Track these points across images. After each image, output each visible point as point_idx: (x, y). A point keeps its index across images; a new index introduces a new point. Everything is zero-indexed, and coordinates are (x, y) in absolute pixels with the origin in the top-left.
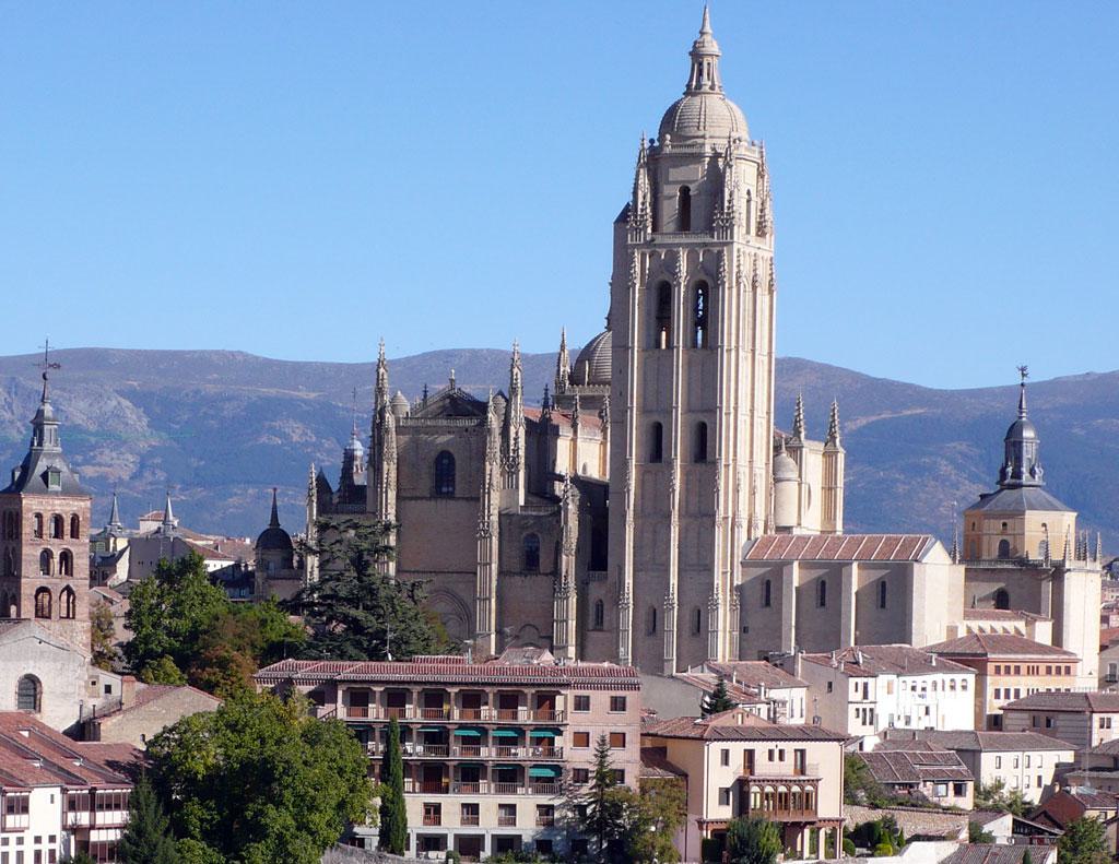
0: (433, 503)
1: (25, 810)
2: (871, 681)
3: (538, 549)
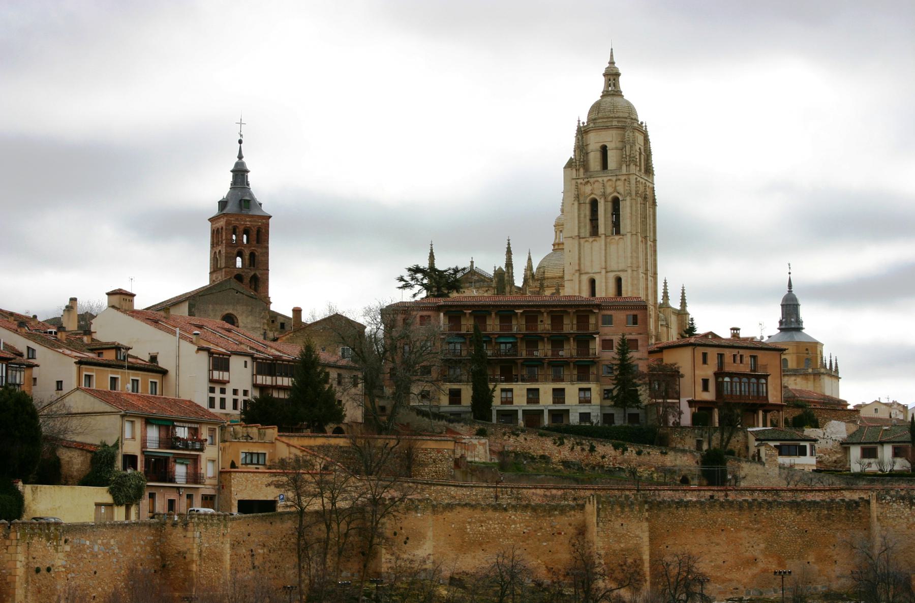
1: (227, 369)
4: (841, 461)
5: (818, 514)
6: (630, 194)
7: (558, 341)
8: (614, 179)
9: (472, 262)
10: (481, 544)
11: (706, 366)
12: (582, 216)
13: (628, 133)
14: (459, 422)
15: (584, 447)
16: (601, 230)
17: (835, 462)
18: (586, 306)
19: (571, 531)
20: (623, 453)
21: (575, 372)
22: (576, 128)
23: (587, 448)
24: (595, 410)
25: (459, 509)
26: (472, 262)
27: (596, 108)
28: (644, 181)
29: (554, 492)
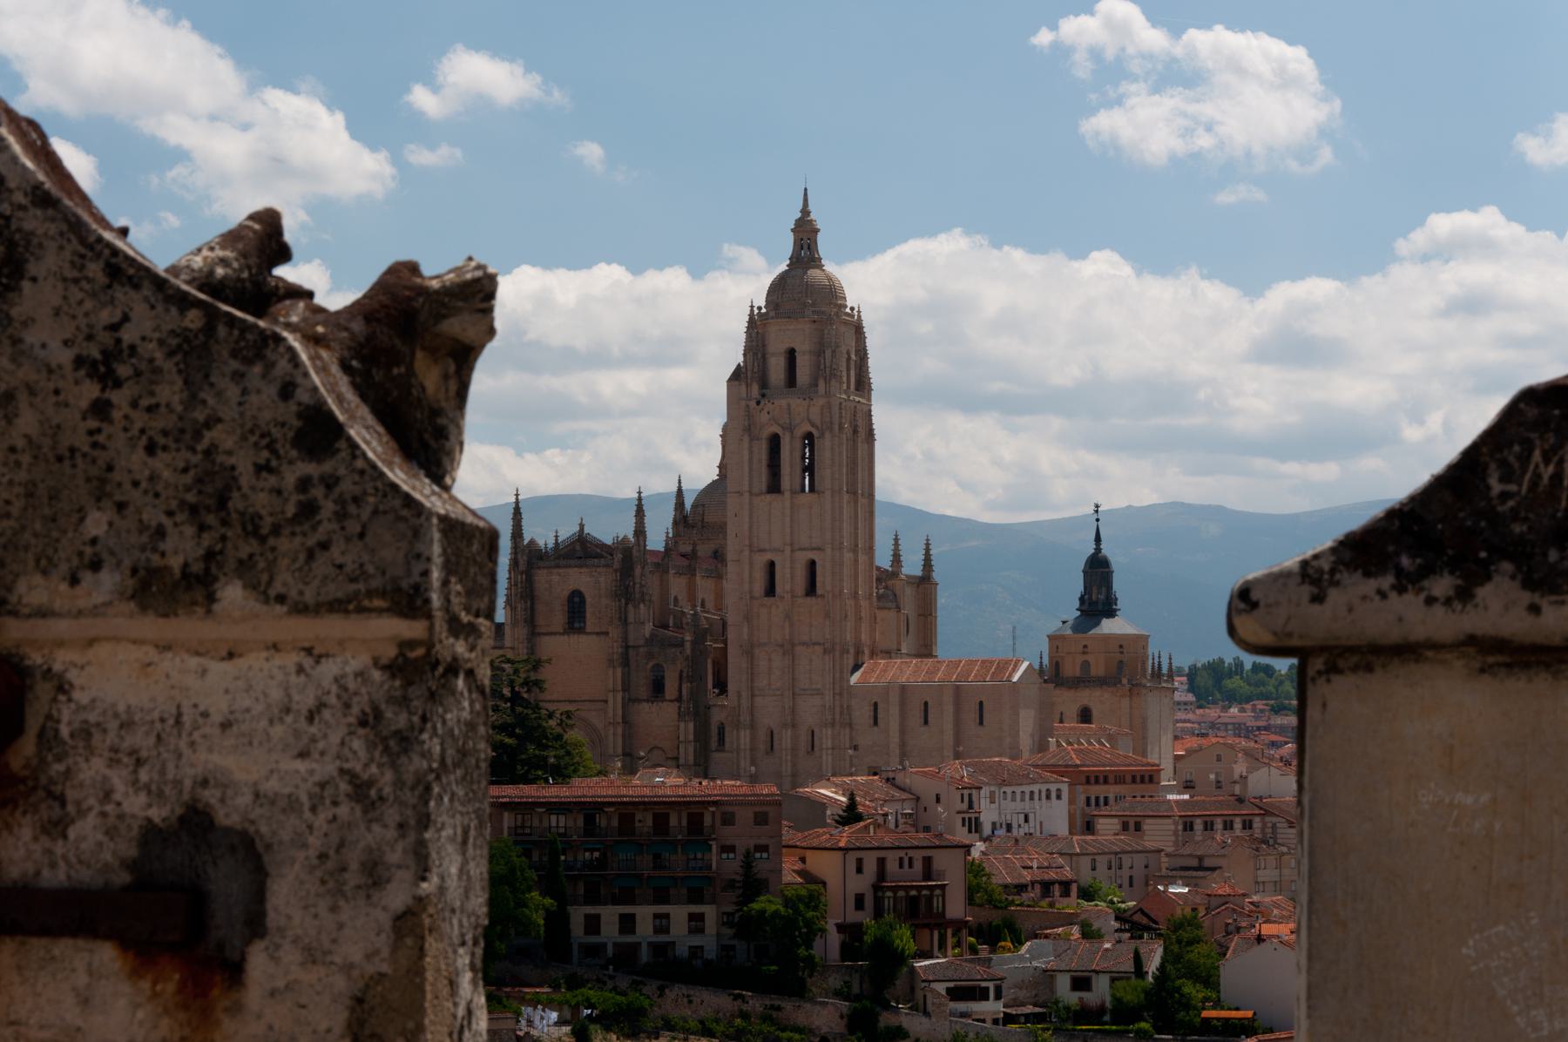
0: (566, 637)
2: (974, 791)
3: (663, 677)
6: (831, 429)
9: (582, 526)
16: (786, 482)
22: (747, 318)
24: (709, 942)
26: (582, 526)
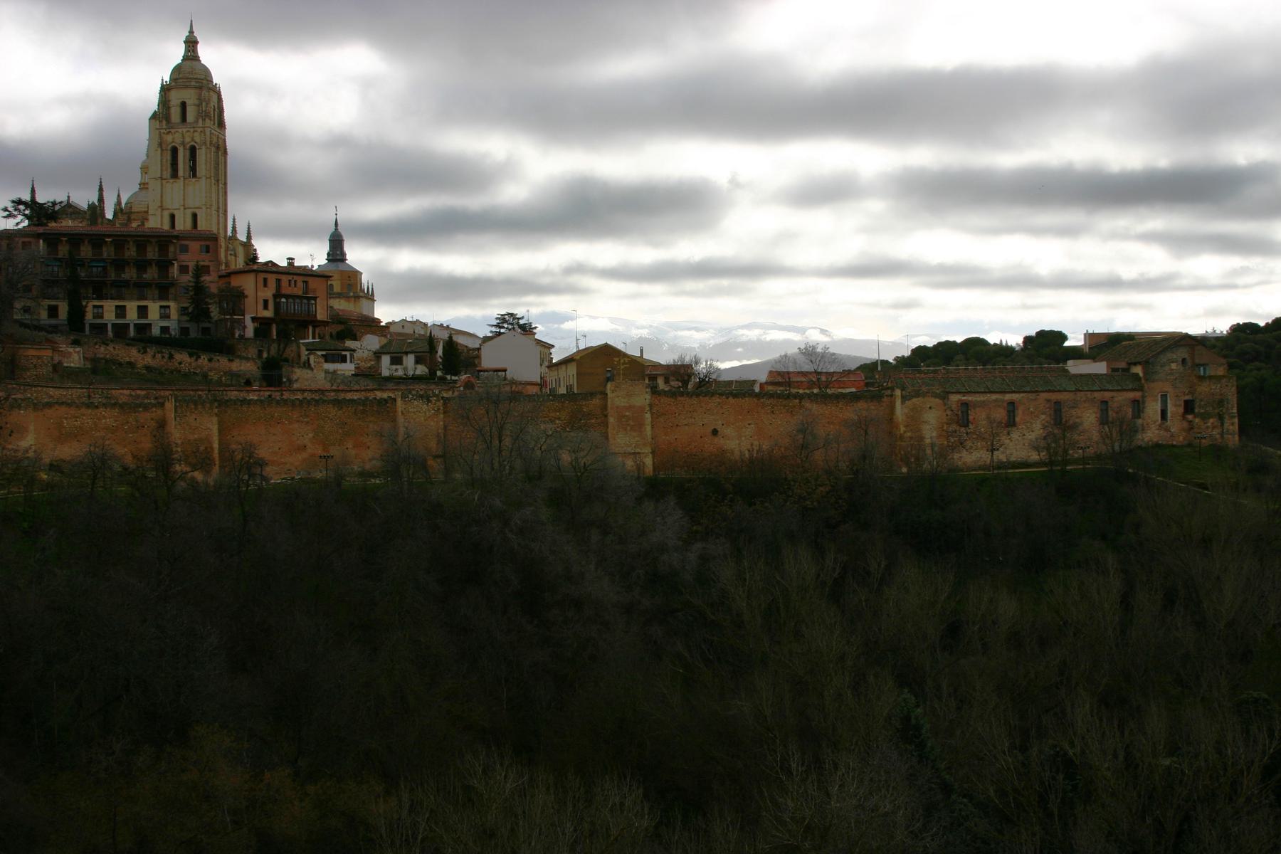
4: (374, 367)
5: (356, 410)
6: (205, 144)
7: (142, 266)
8: (192, 130)
9: (69, 197)
10: (76, 436)
11: (266, 289)
12: (164, 160)
13: (204, 93)
14: (56, 333)
15: (165, 355)
16: (181, 173)
17: (370, 368)
18: (166, 236)
19: (153, 424)
20: (196, 360)
21: (157, 292)
22: (160, 86)
23: (167, 356)
24: (173, 324)
25: (57, 407)
26: (69, 197)
27: (177, 70)
28: (217, 134)
29: (138, 392)
